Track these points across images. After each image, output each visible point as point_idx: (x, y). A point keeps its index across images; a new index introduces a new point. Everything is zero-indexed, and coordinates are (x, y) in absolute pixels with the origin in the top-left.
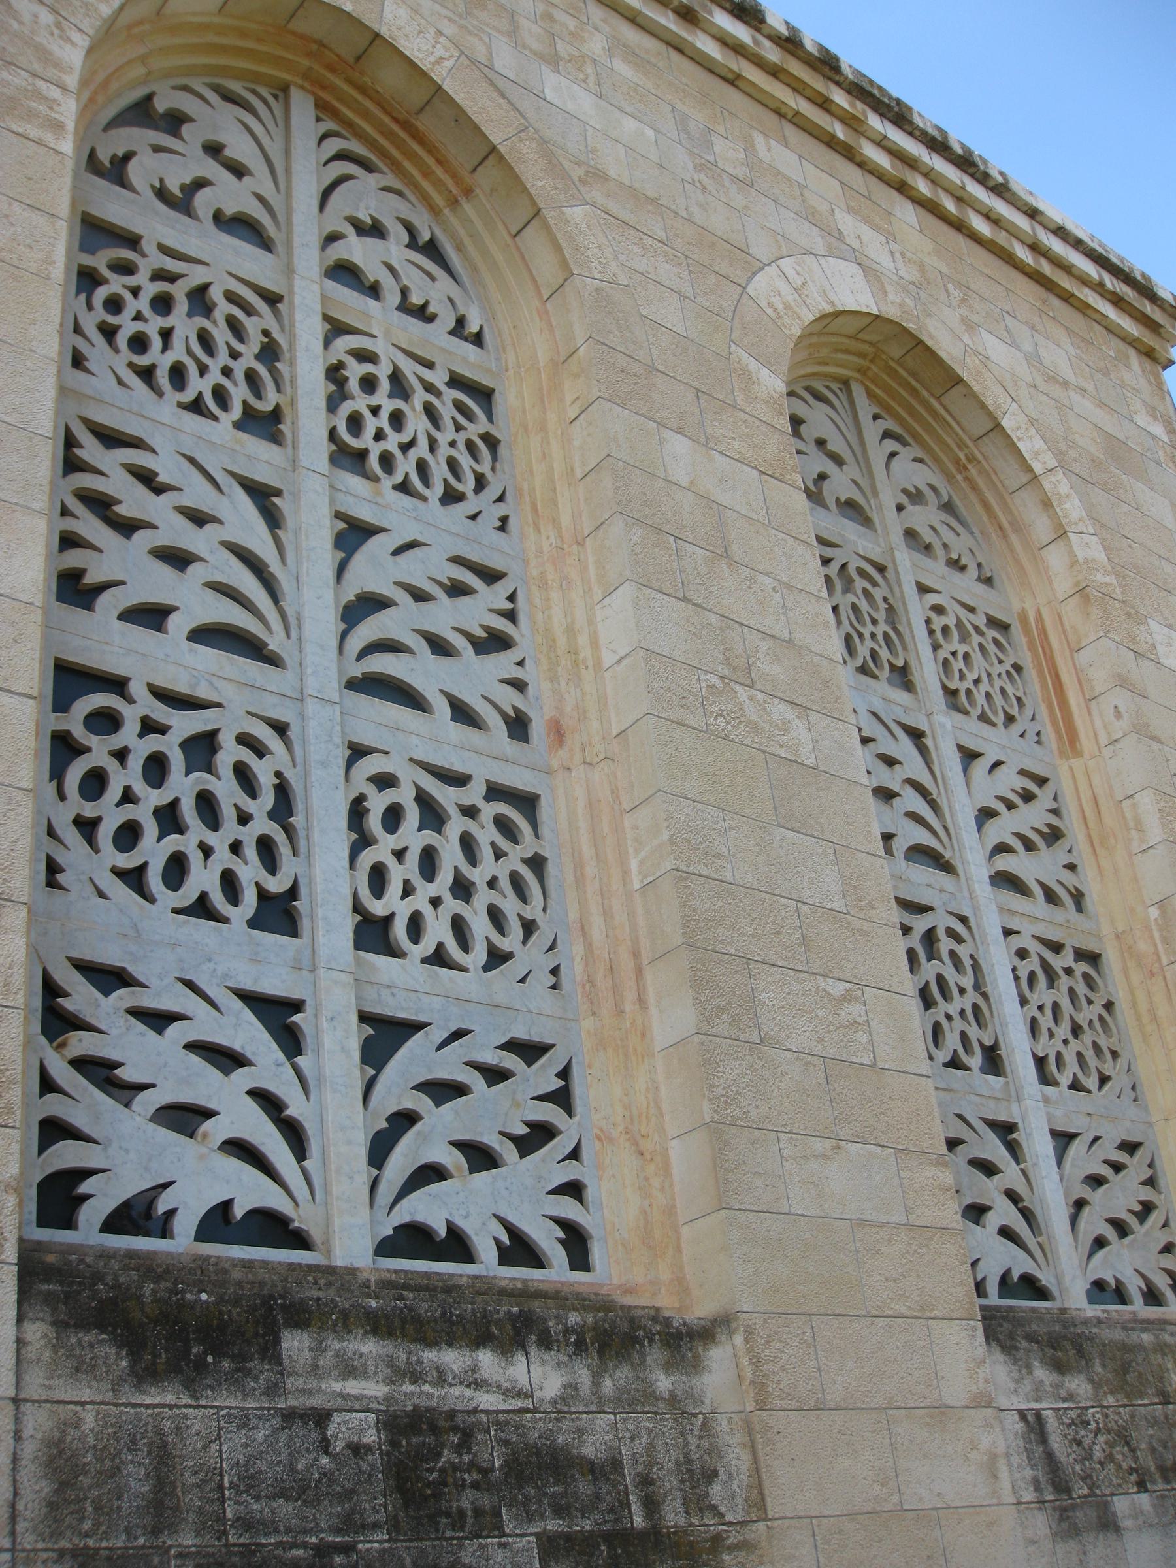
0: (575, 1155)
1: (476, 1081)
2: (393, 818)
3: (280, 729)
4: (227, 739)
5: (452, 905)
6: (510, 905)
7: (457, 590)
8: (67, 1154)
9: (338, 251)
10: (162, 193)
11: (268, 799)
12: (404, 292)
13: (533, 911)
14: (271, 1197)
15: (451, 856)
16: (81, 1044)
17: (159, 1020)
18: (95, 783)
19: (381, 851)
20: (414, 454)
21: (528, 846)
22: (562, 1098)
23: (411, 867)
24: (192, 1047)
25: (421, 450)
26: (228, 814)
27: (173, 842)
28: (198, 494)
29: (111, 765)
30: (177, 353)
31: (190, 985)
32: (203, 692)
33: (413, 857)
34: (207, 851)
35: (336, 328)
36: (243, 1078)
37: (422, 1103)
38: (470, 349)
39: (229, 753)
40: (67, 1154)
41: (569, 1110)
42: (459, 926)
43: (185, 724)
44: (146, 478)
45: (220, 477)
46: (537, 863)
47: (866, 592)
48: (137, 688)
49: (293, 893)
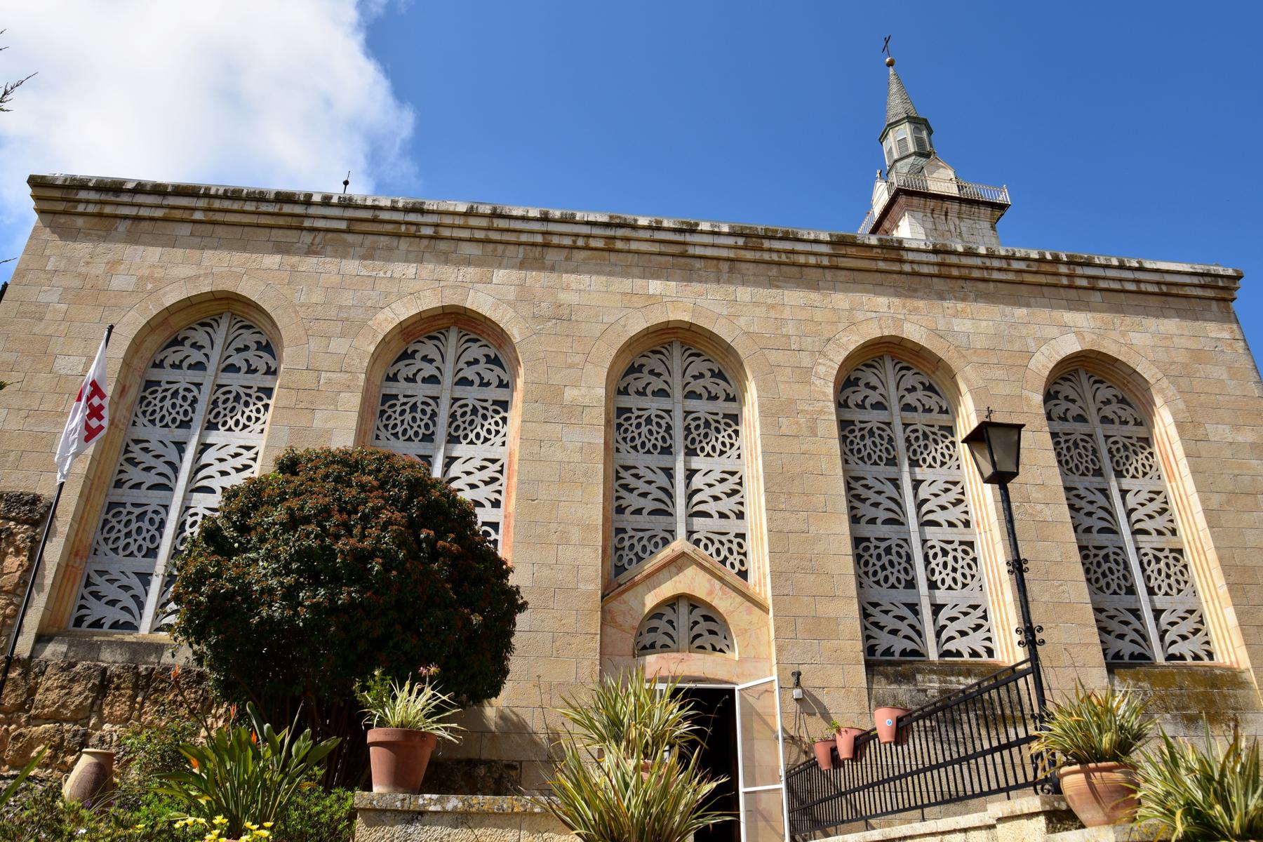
0: (989, 631)
1: (961, 616)
2: (935, 556)
3: (905, 540)
6: (967, 571)
8: (872, 642)
10: (857, 405)
12: (923, 405)
14: (915, 647)
16: (872, 619)
17: (886, 612)
18: (867, 563)
20: (931, 456)
21: (972, 555)
22: (985, 617)
24: (894, 617)
25: (933, 453)
26: (896, 564)
27: (885, 573)
29: (869, 558)
30: (868, 450)
32: (887, 537)
33: (941, 565)
34: (892, 573)
35: (906, 425)
36: (906, 622)
37: (948, 623)
38: (944, 416)
40: (872, 642)
42: (955, 580)
43: (884, 545)
44: (867, 487)
45: (883, 480)
46: (975, 560)
47: (1084, 447)
48: (872, 540)
49: (913, 579)
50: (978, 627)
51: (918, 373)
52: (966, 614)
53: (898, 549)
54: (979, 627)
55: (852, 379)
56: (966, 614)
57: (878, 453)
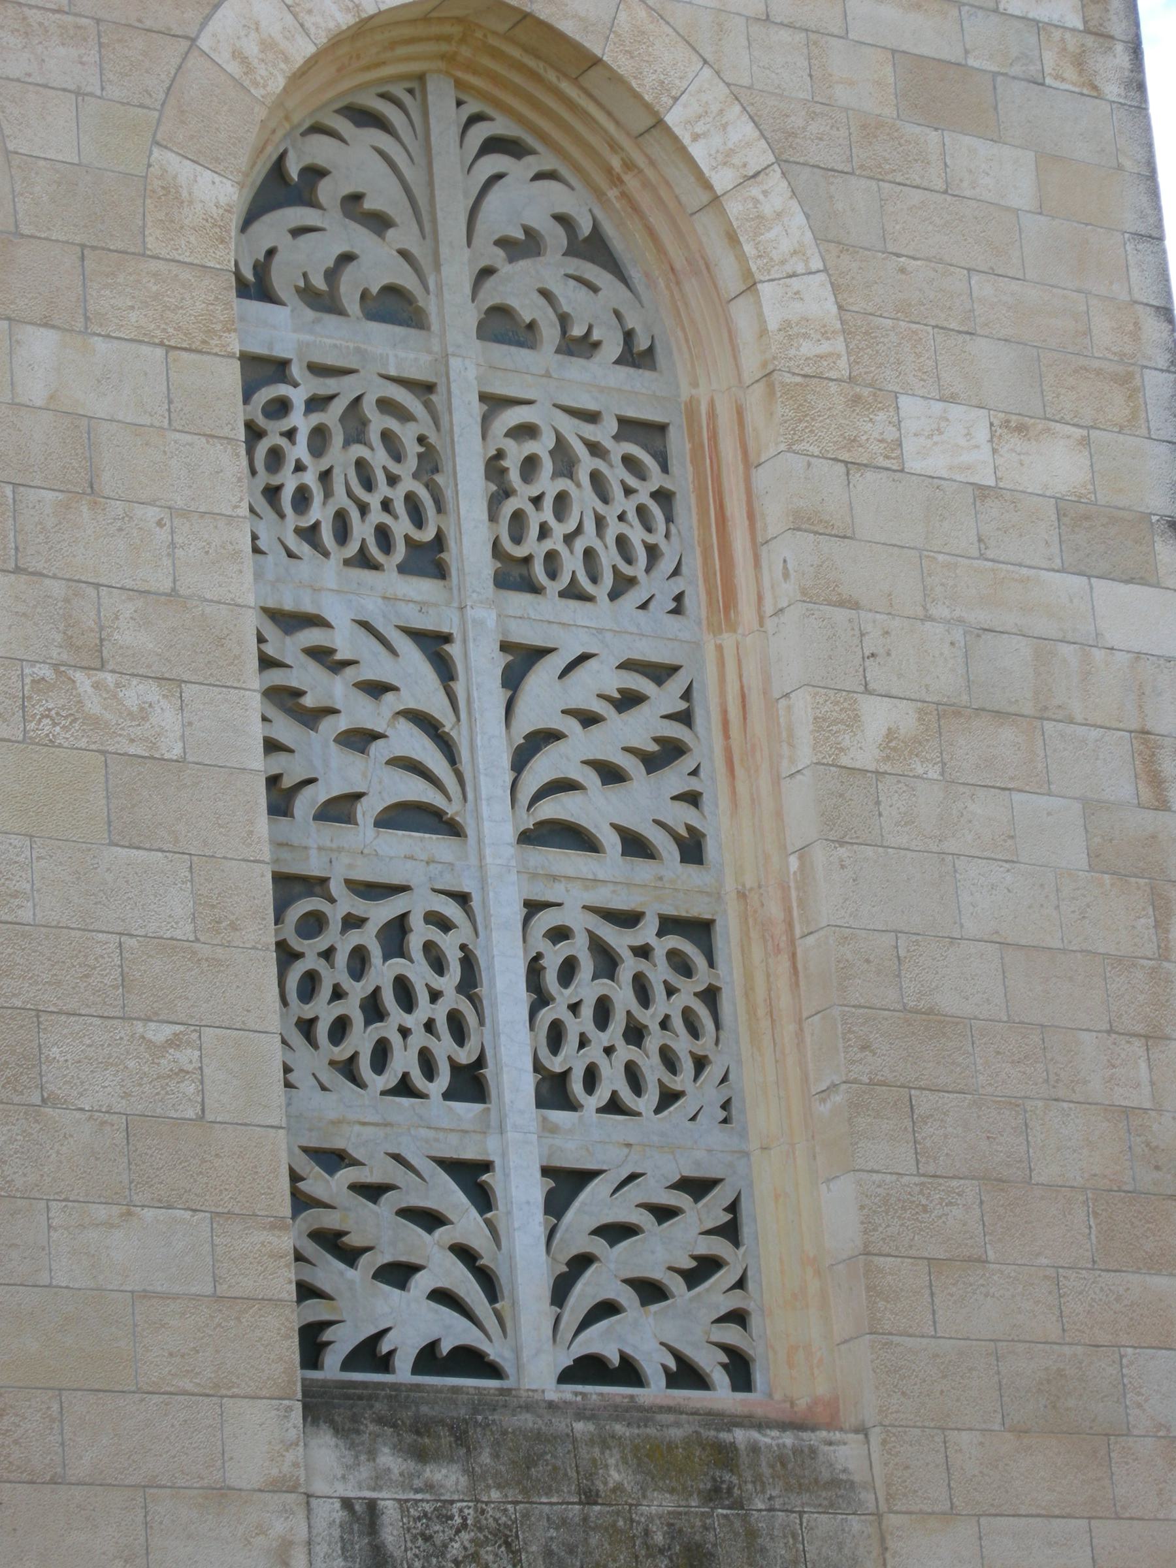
0: (741, 1284)
2: (568, 970)
3: (462, 899)
4: (416, 922)
5: (626, 1052)
6: (682, 1044)
7: (628, 701)
8: (316, 1311)
9: (492, 294)
11: (455, 972)
12: (564, 320)
13: (705, 1045)
15: (623, 997)
17: (372, 1192)
18: (310, 982)
19: (557, 1011)
20: (580, 545)
21: (703, 977)
22: (730, 1231)
23: (586, 1021)
25: (589, 537)
27: (378, 1030)
28: (377, 666)
29: (321, 966)
31: (398, 1158)
33: (587, 1011)
34: (404, 1032)
37: (598, 1246)
39: (420, 933)
41: (736, 1242)
42: (633, 1076)
43: (382, 912)
46: (710, 996)
48: (336, 887)
49: (480, 1062)
50: (706, 1267)
51: (551, 175)
52: (663, 1213)
53: (434, 934)
54: (706, 1267)
55: (293, 170)
56: (663, 1213)
57: (377, 516)
